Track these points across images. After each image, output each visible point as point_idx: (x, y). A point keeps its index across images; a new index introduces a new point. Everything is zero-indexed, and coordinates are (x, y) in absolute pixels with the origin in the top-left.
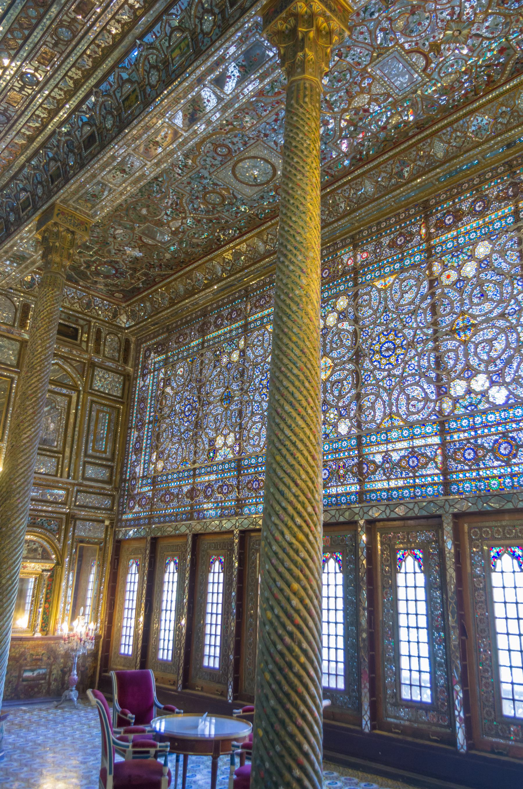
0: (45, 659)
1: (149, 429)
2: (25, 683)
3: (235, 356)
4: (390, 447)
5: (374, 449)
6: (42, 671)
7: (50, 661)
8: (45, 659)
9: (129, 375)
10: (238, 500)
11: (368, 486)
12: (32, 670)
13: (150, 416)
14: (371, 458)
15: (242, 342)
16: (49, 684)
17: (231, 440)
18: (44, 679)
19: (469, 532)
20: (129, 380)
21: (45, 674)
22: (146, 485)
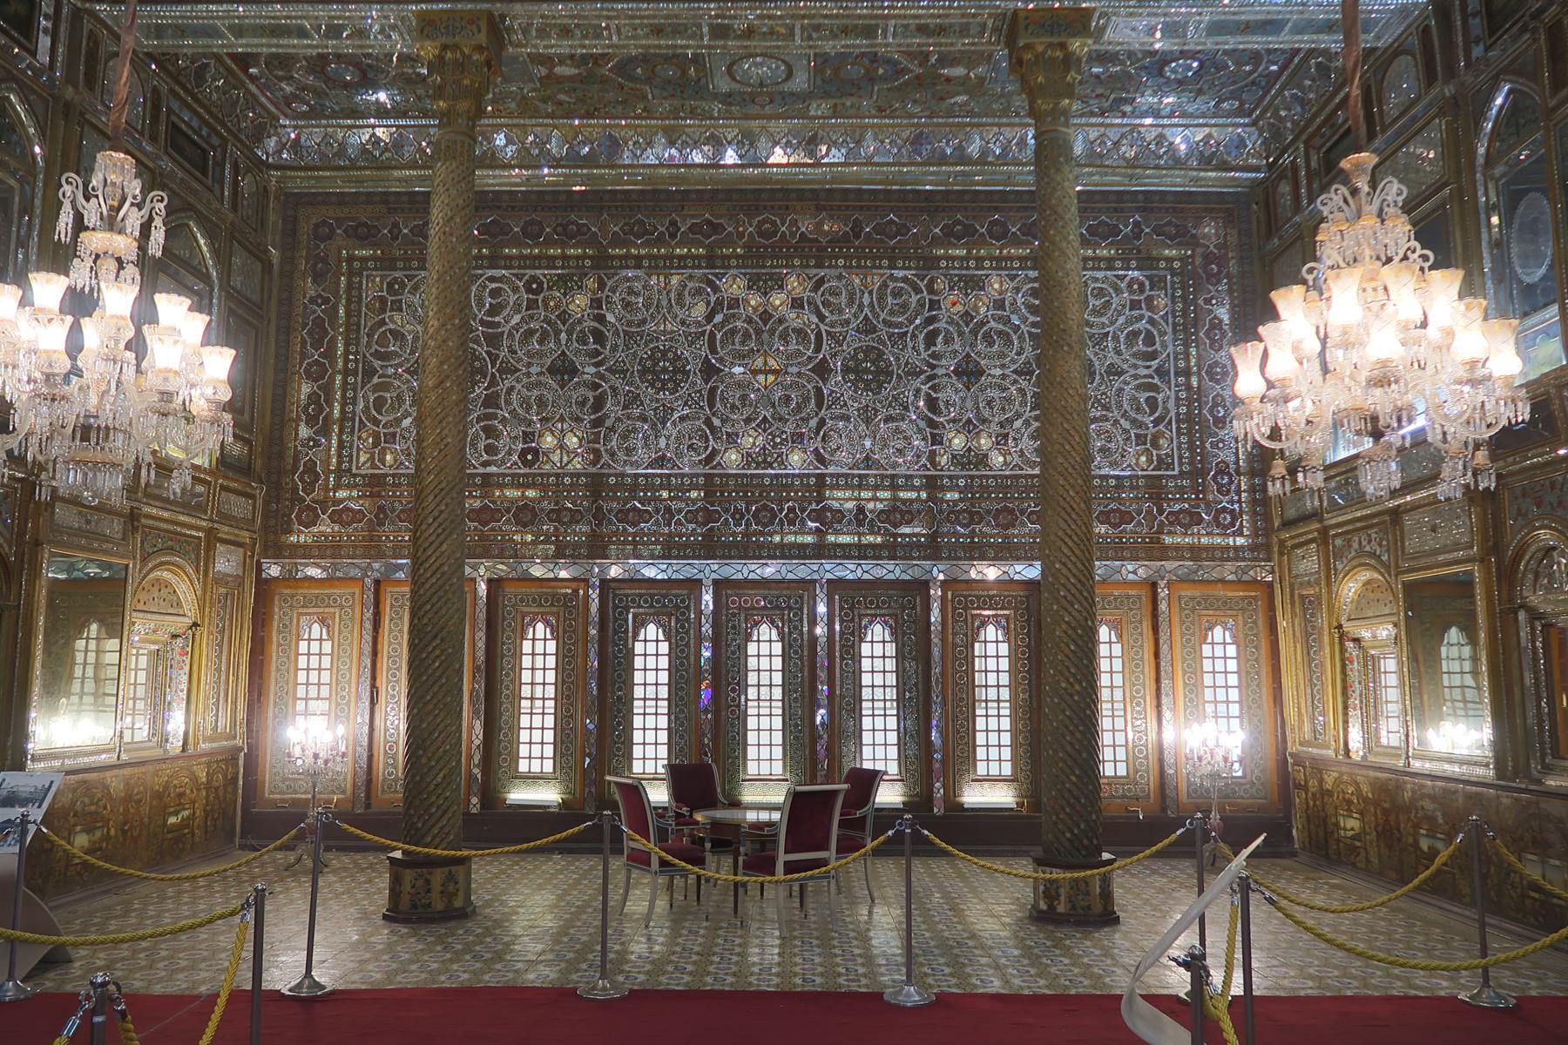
0: (188, 792)
1: (345, 383)
2: (169, 836)
3: (580, 301)
4: (865, 494)
5: (840, 494)
6: (186, 813)
7: (193, 796)
8: (188, 792)
9: (271, 264)
10: (593, 535)
11: (831, 538)
12: (176, 813)
13: (346, 361)
14: (836, 505)
15: (591, 283)
16: (193, 833)
17: (572, 441)
18: (188, 826)
19: (952, 601)
20: (270, 273)
21: (188, 818)
22: (349, 487)
